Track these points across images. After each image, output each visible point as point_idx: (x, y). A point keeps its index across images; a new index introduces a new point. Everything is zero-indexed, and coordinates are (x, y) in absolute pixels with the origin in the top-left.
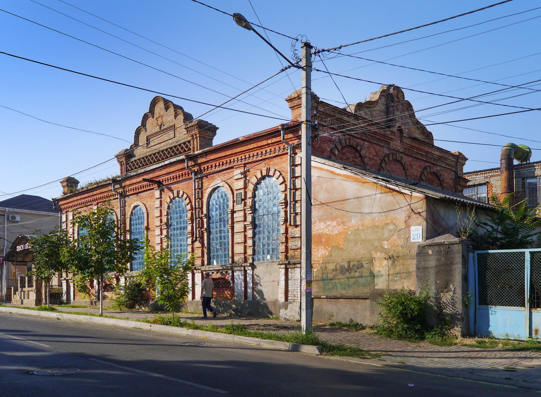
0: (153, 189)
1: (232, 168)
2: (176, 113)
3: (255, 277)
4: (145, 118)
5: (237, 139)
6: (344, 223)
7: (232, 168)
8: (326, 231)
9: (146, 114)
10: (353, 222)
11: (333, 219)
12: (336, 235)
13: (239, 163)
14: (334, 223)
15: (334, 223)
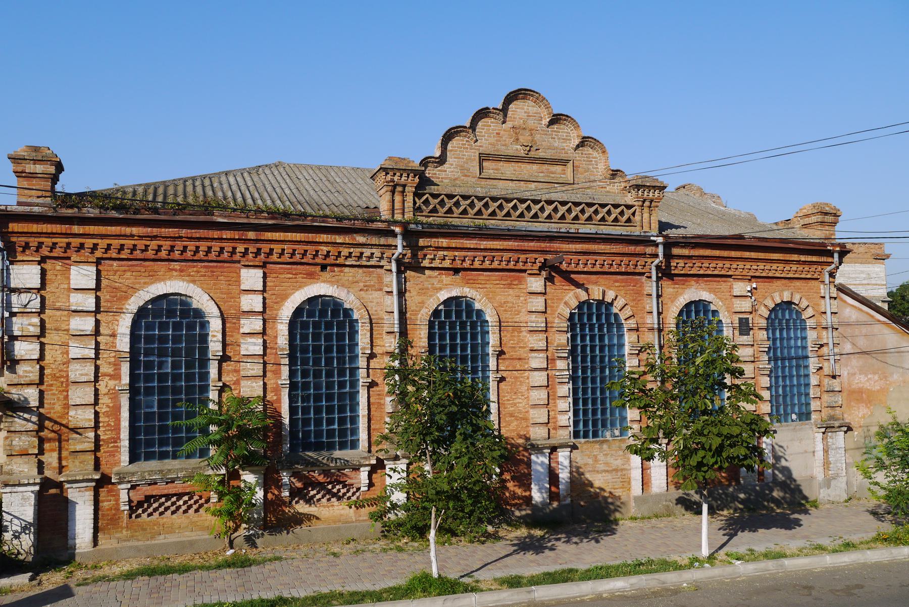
0: (525, 271)
1: (730, 276)
2: (582, 142)
3: (776, 447)
4: (482, 114)
5: (740, 237)
6: (886, 377)
7: (730, 276)
8: (867, 386)
9: (487, 108)
10: (895, 376)
11: (874, 373)
12: (878, 391)
13: (744, 273)
14: (876, 377)
15: (876, 377)
